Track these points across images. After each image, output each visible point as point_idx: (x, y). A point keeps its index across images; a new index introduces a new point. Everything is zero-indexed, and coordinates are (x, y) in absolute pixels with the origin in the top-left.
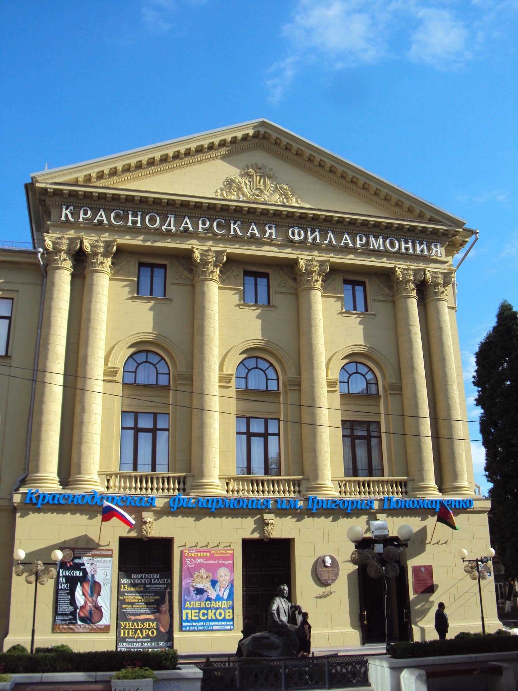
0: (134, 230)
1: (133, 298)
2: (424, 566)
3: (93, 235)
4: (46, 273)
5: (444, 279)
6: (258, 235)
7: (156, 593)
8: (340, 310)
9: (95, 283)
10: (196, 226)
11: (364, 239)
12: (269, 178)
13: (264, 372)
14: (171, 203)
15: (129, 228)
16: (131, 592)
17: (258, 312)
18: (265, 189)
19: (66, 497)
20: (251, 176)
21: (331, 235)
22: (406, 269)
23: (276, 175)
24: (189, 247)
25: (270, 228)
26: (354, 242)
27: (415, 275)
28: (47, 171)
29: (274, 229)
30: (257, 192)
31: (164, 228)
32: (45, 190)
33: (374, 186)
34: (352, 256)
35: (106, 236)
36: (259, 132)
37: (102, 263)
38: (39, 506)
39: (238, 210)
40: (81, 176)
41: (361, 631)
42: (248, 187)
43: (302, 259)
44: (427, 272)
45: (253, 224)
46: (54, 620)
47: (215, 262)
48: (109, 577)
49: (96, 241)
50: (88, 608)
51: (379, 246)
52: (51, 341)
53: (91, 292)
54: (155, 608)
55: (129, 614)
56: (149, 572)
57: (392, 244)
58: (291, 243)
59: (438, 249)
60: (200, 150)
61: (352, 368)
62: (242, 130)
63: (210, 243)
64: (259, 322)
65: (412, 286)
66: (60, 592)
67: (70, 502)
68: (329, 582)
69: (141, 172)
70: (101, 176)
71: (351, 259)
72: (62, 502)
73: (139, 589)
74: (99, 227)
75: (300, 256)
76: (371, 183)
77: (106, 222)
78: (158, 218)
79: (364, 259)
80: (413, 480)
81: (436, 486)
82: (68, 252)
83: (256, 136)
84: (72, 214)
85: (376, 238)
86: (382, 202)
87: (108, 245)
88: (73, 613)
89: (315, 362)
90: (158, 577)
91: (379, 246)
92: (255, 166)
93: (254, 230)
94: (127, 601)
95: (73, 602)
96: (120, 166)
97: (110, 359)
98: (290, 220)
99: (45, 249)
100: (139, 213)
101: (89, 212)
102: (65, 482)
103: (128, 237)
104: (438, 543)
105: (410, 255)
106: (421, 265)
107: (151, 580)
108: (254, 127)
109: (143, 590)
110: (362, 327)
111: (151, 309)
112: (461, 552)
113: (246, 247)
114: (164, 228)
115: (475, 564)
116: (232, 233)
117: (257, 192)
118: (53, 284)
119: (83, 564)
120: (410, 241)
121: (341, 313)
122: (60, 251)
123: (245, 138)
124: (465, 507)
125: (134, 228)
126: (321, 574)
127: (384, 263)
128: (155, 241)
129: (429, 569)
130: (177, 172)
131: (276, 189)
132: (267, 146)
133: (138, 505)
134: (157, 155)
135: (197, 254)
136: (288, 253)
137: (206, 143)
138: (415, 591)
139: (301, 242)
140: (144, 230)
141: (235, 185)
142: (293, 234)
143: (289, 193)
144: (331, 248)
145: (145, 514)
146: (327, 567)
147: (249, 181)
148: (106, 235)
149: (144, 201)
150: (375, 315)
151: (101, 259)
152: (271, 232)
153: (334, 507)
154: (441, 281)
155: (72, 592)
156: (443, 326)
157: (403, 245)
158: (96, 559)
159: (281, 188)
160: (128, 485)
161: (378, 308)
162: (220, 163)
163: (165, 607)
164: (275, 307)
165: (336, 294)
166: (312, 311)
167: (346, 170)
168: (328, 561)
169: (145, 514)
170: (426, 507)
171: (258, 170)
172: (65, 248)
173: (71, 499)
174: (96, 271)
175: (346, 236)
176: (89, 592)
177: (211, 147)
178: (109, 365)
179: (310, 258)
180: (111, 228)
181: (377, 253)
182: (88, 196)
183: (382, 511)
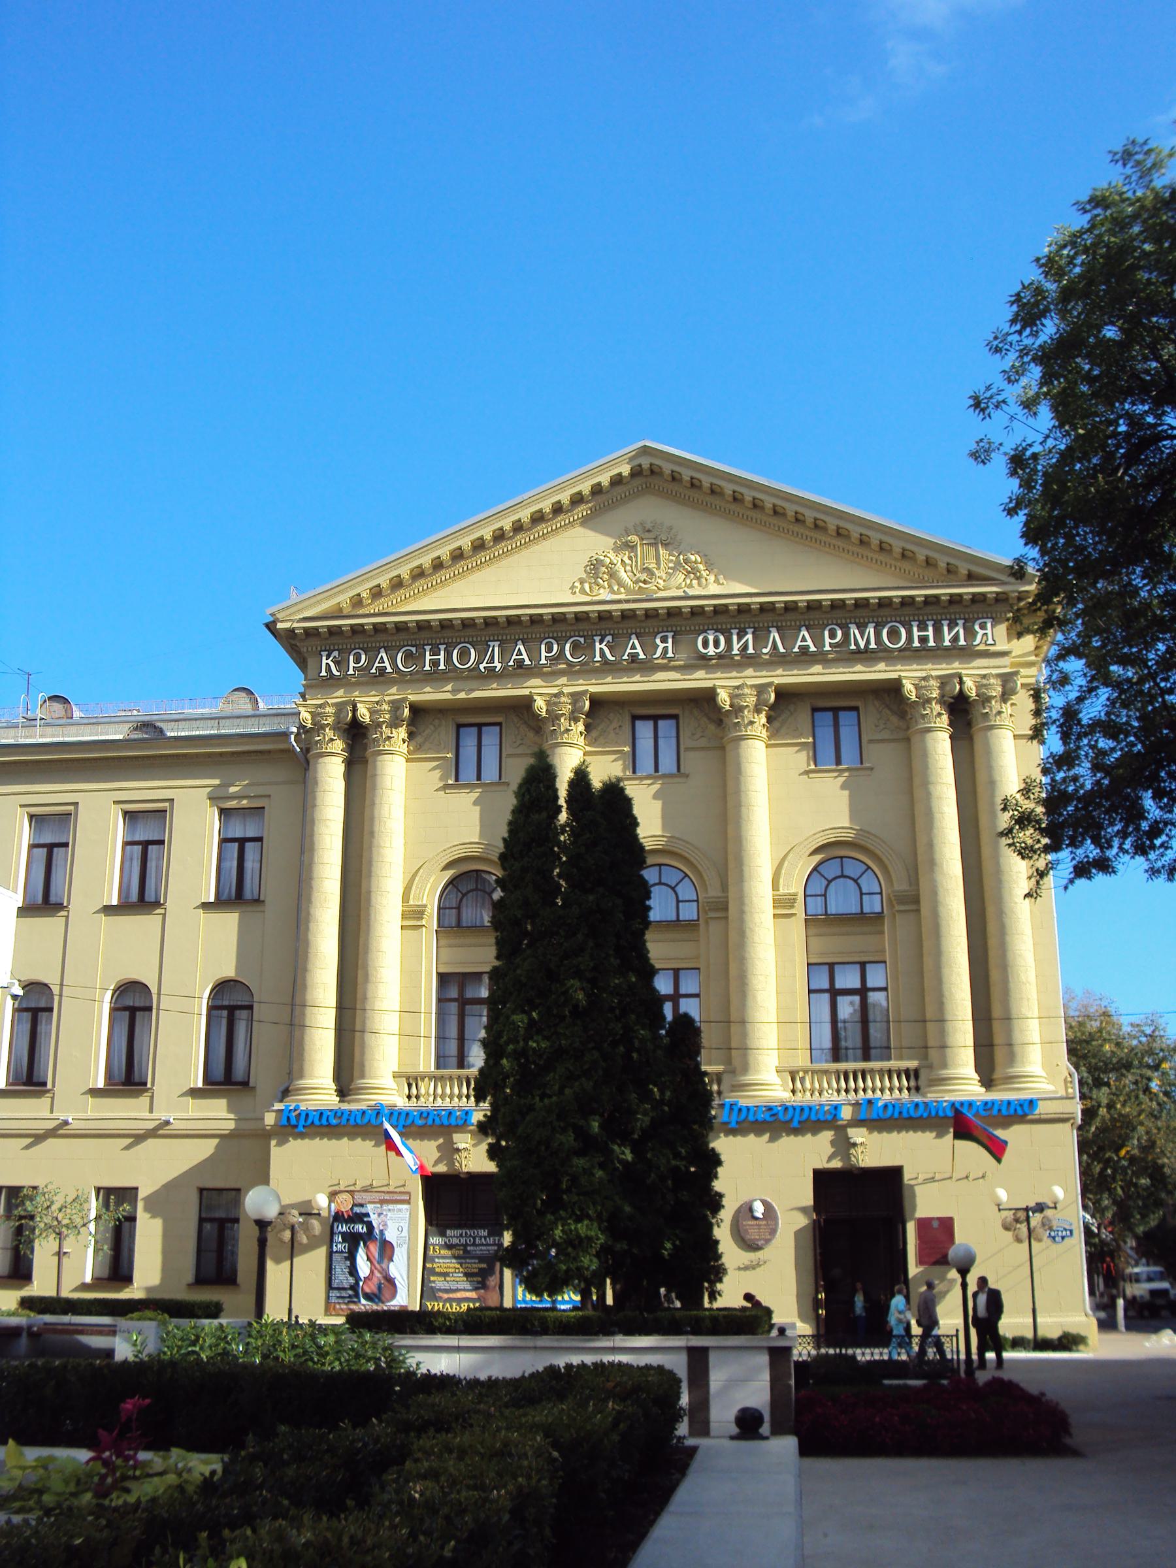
0: (435, 677)
1: (446, 787)
2: (939, 1219)
3: (373, 693)
4: (308, 762)
5: (1003, 686)
6: (642, 656)
7: (481, 1259)
8: (804, 767)
9: (379, 772)
10: (534, 654)
11: (839, 633)
12: (666, 545)
13: (673, 889)
14: (489, 623)
15: (428, 673)
16: (444, 1257)
17: (657, 787)
18: (658, 568)
19: (339, 1114)
20: (633, 548)
21: (775, 635)
22: (924, 679)
23: (679, 537)
24: (526, 692)
25: (664, 640)
26: (819, 642)
27: (942, 686)
28: (294, 597)
29: (670, 640)
30: (644, 576)
31: (482, 667)
32: (291, 631)
33: (855, 531)
34: (818, 668)
35: (393, 693)
36: (640, 466)
37: (389, 738)
38: (301, 1129)
39: (604, 617)
40: (344, 599)
41: (814, 1325)
42: (628, 568)
43: (723, 687)
44: (965, 679)
45: (633, 636)
46: (328, 1297)
47: (573, 712)
48: (405, 1233)
49: (377, 703)
50: (375, 1281)
51: (868, 642)
52: (315, 875)
53: (374, 787)
54: (478, 1282)
55: (440, 1290)
56: (472, 1227)
57: (894, 635)
58: (703, 661)
59: (989, 631)
60: (538, 518)
61: (832, 870)
62: (608, 469)
63: (563, 680)
64: (658, 804)
65: (937, 708)
66: (336, 1257)
67: (344, 1122)
68: (760, 1243)
69: (442, 574)
70: (377, 593)
71: (816, 675)
72: (334, 1122)
73: (456, 1252)
74: (381, 678)
75: (718, 683)
76: (849, 526)
77: (389, 670)
78: (472, 651)
79: (841, 670)
80: (930, 1067)
81: (976, 1077)
82: (335, 728)
83: (636, 473)
84: (336, 662)
85: (862, 627)
86: (875, 556)
87: (396, 706)
88: (354, 1288)
89: (746, 869)
90: (486, 1234)
91: (868, 642)
92: (639, 529)
93: (635, 647)
94: (437, 1270)
95: (353, 1271)
96: (404, 571)
97: (413, 891)
98: (699, 620)
99: (301, 727)
100: (442, 647)
101: (363, 657)
102: (343, 1092)
103: (428, 689)
104: (967, 1177)
105: (931, 649)
106: (955, 667)
107: (474, 1238)
108: (631, 459)
109: (463, 1254)
110: (846, 793)
111: (475, 803)
112: (994, 1195)
113: (625, 679)
114: (482, 667)
115: (1022, 1215)
116: (598, 658)
117: (644, 576)
118: (316, 783)
119: (367, 1215)
120: (930, 623)
121: (807, 773)
122: (323, 727)
123: (617, 481)
124: (1022, 1113)
125: (435, 672)
126: (746, 1231)
127: (880, 672)
128: (473, 690)
129: (947, 1225)
130: (504, 562)
131: (677, 566)
132: (657, 489)
133: (446, 1122)
134: (465, 542)
135: (540, 704)
136: (698, 680)
137: (546, 506)
138: (921, 1261)
139: (720, 656)
140: (451, 674)
141: (604, 569)
142: (705, 644)
143: (701, 567)
144: (779, 660)
145: (456, 1137)
146: (757, 1219)
147: (630, 558)
148: (394, 690)
149: (445, 625)
150: (872, 769)
151: (386, 731)
152: (664, 646)
153: (769, 1119)
154: (996, 690)
155: (352, 1257)
156: (998, 778)
157: (916, 633)
158: (385, 1207)
159: (686, 561)
160: (448, 1091)
161: (882, 755)
162: (579, 531)
163: (493, 1281)
164: (687, 776)
165: (801, 736)
166: (742, 779)
167: (800, 510)
168: (759, 1209)
169: (456, 1137)
170: (941, 1114)
171: (647, 535)
172: (330, 720)
173: (345, 1116)
174: (381, 753)
175: (804, 632)
176: (377, 1256)
177: (558, 509)
178: (411, 902)
179: (737, 683)
180: (402, 679)
181: (864, 655)
182: (356, 630)
183: (857, 1122)
